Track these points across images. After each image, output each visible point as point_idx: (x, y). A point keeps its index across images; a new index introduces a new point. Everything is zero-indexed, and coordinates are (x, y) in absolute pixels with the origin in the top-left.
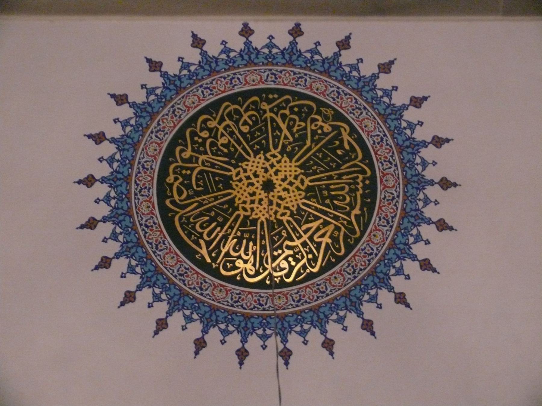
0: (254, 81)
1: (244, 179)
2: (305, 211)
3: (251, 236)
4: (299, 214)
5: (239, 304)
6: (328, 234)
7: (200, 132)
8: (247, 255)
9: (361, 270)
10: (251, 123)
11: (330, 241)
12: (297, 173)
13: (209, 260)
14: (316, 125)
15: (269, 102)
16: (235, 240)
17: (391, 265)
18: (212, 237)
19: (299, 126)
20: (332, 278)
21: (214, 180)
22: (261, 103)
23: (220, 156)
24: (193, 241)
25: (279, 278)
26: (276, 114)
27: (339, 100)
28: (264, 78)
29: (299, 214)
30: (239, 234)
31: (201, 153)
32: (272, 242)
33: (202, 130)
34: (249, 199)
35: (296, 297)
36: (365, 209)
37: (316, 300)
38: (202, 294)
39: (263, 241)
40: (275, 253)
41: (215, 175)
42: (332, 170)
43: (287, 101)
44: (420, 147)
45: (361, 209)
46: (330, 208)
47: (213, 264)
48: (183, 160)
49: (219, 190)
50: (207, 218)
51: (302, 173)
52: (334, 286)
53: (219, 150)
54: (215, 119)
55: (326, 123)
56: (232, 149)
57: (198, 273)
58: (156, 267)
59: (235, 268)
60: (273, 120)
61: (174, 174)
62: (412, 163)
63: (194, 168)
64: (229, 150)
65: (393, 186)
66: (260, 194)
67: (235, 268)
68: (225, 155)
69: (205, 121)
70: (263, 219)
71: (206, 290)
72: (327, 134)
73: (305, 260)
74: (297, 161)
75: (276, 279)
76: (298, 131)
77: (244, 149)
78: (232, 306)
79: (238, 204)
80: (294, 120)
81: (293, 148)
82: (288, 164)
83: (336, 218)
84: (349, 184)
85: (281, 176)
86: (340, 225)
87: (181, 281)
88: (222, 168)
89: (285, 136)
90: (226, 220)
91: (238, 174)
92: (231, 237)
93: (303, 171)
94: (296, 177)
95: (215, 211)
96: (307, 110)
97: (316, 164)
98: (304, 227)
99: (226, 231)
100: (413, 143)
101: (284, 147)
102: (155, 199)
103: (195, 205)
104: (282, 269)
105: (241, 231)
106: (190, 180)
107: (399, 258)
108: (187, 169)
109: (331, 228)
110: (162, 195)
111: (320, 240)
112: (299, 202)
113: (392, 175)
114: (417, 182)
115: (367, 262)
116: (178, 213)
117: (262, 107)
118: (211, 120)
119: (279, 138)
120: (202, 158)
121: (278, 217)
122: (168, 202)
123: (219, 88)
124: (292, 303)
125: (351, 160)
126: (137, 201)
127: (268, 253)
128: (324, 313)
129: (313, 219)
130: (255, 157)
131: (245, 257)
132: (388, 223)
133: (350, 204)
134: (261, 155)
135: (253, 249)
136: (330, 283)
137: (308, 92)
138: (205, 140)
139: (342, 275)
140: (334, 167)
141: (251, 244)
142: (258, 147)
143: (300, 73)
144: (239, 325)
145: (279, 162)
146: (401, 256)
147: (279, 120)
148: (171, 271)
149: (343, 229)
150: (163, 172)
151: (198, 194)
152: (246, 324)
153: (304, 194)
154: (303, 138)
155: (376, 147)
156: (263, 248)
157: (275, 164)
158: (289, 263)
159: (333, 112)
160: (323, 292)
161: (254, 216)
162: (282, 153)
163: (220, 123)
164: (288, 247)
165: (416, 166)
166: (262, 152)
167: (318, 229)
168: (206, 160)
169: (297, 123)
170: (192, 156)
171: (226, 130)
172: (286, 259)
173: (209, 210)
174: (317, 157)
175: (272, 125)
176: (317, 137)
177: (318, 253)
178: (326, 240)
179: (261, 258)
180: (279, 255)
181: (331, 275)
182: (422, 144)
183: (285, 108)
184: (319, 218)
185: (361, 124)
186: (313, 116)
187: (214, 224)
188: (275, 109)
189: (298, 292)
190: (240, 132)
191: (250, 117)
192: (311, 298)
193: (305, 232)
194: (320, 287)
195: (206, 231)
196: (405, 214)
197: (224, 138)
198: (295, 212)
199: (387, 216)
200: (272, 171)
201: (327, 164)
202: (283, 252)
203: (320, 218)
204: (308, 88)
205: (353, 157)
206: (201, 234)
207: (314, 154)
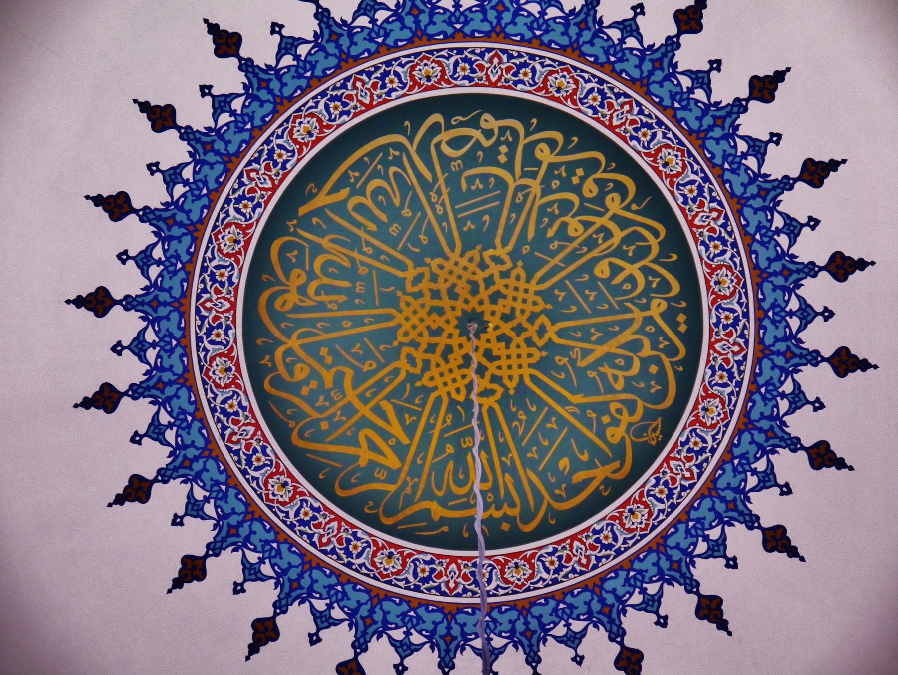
0: (718, 283)
1: (486, 274)
2: (423, 405)
3: (358, 296)
4: (415, 392)
5: (209, 283)
6: (375, 457)
7: (596, 181)
8: (317, 293)
9: (310, 536)
11: (362, 463)
12: (506, 381)
13: (302, 210)
14: (619, 411)
15: (669, 316)
16: (346, 264)
17: (334, 599)
18: (353, 214)
20: (283, 478)
21: (483, 213)
22: (668, 300)
23: (539, 222)
24: (345, 175)
25: (270, 365)
27: (684, 454)
28: (725, 303)
29: (415, 392)
30: (363, 271)
31: (546, 181)
32: (348, 343)
34: (443, 287)
35: (231, 406)
36: (445, 529)
37: (230, 450)
38: (228, 201)
39: (349, 324)
40: (324, 351)
41: (495, 214)
42: (522, 452)
44: (608, 626)
45: (443, 521)
46: (435, 455)
47: (295, 221)
48: (530, 148)
49: (461, 223)
50: (397, 201)
51: (507, 389)
52: (266, 483)
53: (553, 218)
54: (627, 208)
55: (627, 431)
56: (554, 246)
57: (274, 189)
58: (292, 100)
61: (500, 128)
62: (570, 613)
64: (552, 240)
65: (506, 581)
66: (453, 308)
67: (287, 268)
68: (541, 233)
69: (620, 189)
70: (399, 318)
71: (237, 210)
72: (601, 434)
74: (533, 378)
75: (267, 358)
76: (603, 376)
78: (204, 269)
79: (429, 265)
80: (628, 365)
82: (525, 361)
83: (415, 471)
85: (498, 349)
86: (399, 483)
87: (257, 155)
88: (509, 229)
89: (592, 351)
90: (393, 242)
91: (497, 260)
93: (512, 392)
94: (495, 379)
95: (414, 216)
96: (652, 391)
98: (387, 407)
99: (368, 244)
100: (614, 610)
101: (565, 351)
102: (446, 91)
104: (290, 369)
105: (370, 274)
108: (511, 155)
109: (392, 461)
113: (532, 576)
114: (528, 629)
115: (329, 548)
116: (411, 140)
117: (654, 302)
118: (622, 200)
119: (586, 339)
120: (535, 186)
121: (405, 350)
122: (437, 118)
123: (701, 214)
124: (219, 399)
125: (550, 488)
126: (444, 53)
128: (205, 469)
129: (408, 423)
130: (537, 293)
131: (311, 290)
133: (450, 495)
135: (330, 302)
136: (271, 476)
138: (577, 189)
139: (292, 499)
140: (529, 455)
141: (343, 298)
142: (560, 299)
143: (741, 373)
144: (162, 289)
145: (529, 342)
146: (358, 617)
147: (628, 336)
148: (280, 131)
149: (392, 488)
151: (453, 180)
152: (165, 304)
153: (461, 398)
154: (588, 387)
155: (587, 537)
156: (335, 324)
157: (524, 335)
158: (306, 382)
159: (654, 443)
160: (249, 463)
162: (550, 346)
163: (615, 218)
164: (339, 379)
165: (563, 622)
166: (549, 306)
167: (385, 435)
168: (529, 193)
169: (620, 374)
170: (539, 163)
171: (597, 232)
173: (416, 206)
174: (547, 419)
175: (612, 324)
176: (593, 415)
178: (365, 456)
179: (312, 322)
180: (320, 360)
181: (290, 475)
182: (615, 628)
183: (654, 347)
184: (411, 436)
185: (635, 501)
186: (640, 404)
187: (383, 217)
188: (650, 329)
189: (244, 409)
190: (596, 260)
191: (631, 279)
192: (235, 439)
193: (378, 411)
194: (259, 455)
195: (369, 202)
197: (581, 228)
198: (418, 384)
199: (439, 575)
200: (506, 328)
201: (534, 440)
202: (328, 368)
203: (411, 436)
204: (705, 390)
205: (557, 492)
207: (552, 412)
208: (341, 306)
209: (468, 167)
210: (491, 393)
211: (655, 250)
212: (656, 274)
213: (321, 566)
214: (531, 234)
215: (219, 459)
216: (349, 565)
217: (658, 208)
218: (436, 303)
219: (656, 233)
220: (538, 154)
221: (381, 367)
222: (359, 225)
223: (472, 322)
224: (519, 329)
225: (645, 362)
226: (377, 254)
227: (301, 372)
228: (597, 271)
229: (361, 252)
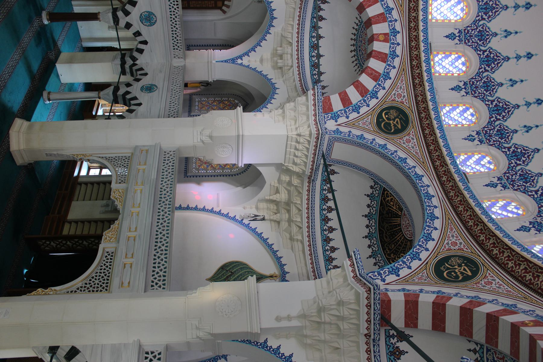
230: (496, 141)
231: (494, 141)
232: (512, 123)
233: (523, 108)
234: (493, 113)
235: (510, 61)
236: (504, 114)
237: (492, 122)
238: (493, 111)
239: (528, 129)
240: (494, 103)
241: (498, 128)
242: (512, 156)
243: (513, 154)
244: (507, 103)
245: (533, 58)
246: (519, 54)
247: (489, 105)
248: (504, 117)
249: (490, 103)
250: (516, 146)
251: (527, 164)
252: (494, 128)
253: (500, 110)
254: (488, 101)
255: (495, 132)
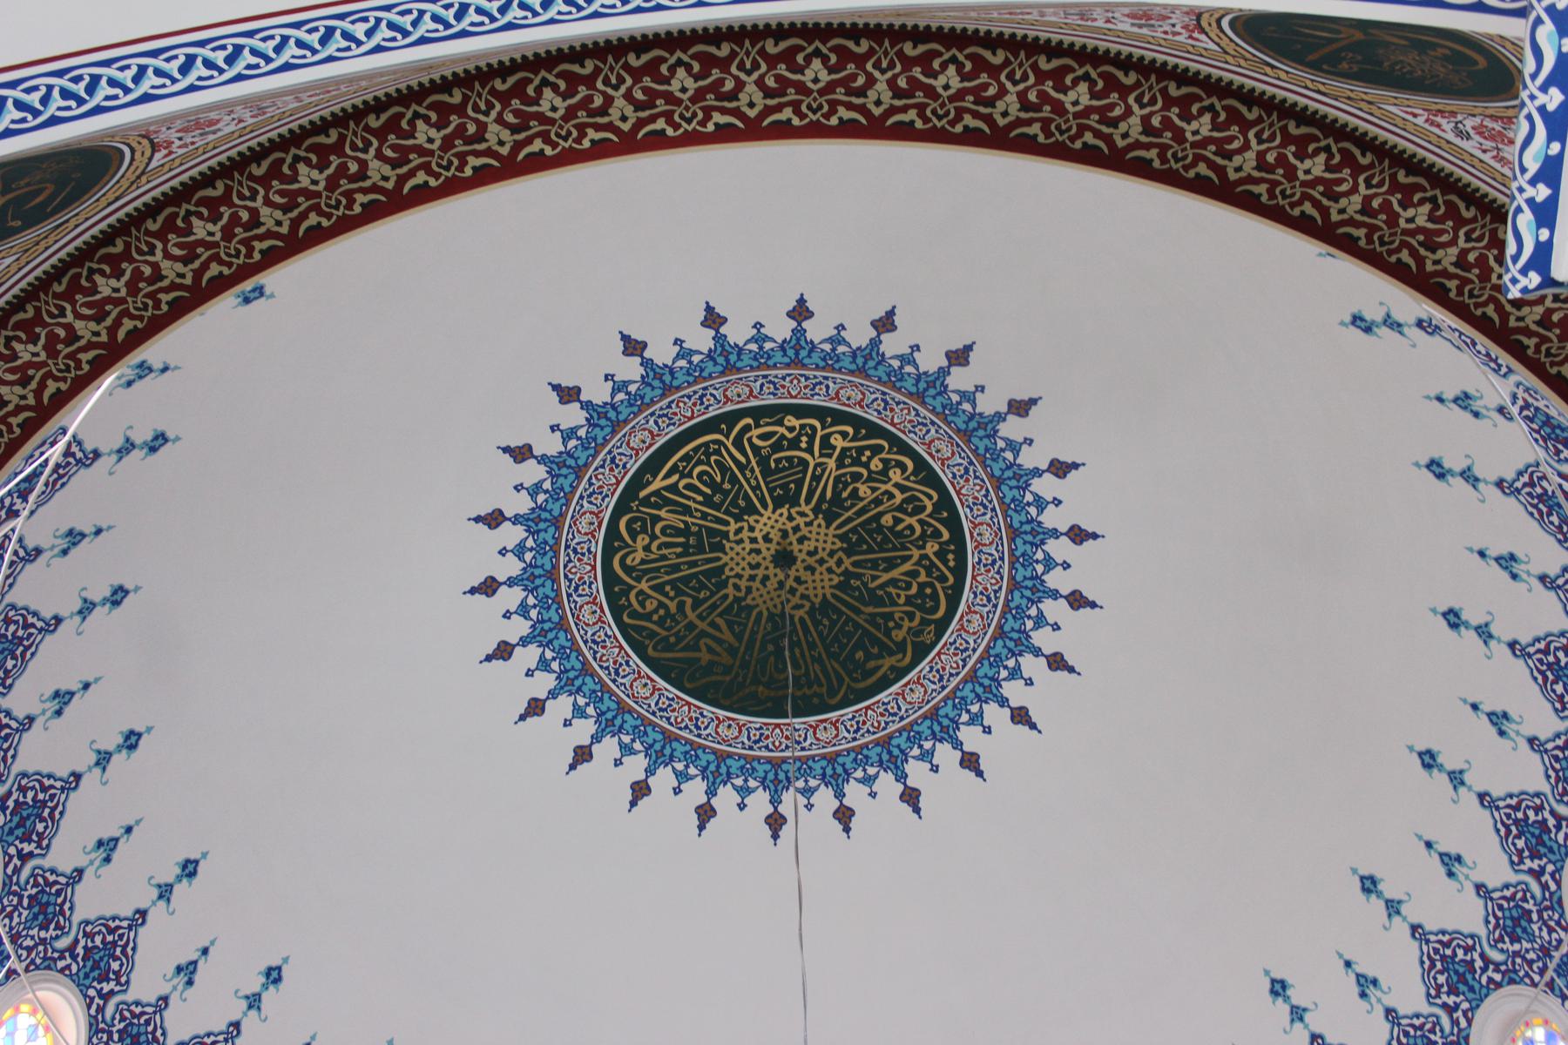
2: (748, 618)
4: (741, 609)
6: (716, 658)
8: (659, 548)
10: (899, 528)
11: (703, 663)
13: (642, 494)
14: (902, 619)
15: (941, 554)
19: (899, 596)
26: (918, 563)
29: (741, 609)
30: (694, 529)
32: (686, 580)
33: (885, 462)
40: (668, 588)
43: (943, 579)
49: (771, 491)
50: (718, 479)
53: (846, 485)
54: (907, 479)
59: (634, 535)
60: (906, 559)
63: (812, 454)
67: (634, 535)
68: (836, 493)
69: (903, 468)
73: (665, 633)
76: (889, 595)
77: (849, 520)
80: (909, 586)
81: (858, 588)
83: (744, 665)
84: (807, 673)
90: (717, 507)
92: (687, 519)
97: (833, 623)
101: (858, 576)
102: (754, 403)
103: (743, 460)
106: (789, 449)
107: (704, 770)
108: (811, 443)
110: (758, 413)
111: (704, 649)
112: (763, 607)
117: (929, 545)
120: (831, 463)
125: (849, 674)
127: (667, 578)
131: (654, 547)
132: (756, 742)
134: (839, 544)
137: (962, 607)
138: (866, 465)
141: (679, 550)
145: (830, 570)
147: (907, 567)
150: (800, 411)
151: (763, 462)
153: (778, 611)
156: (676, 568)
161: (728, 545)
162: (846, 573)
163: (896, 485)
164: (681, 605)
167: (720, 641)
170: (834, 448)
172: (661, 605)
173: (734, 480)
175: (896, 558)
177: (682, 650)
178: (705, 657)
179: (658, 569)
180: (666, 595)
183: (929, 574)
190: (881, 514)
191: (910, 527)
193: (713, 624)
196: (777, 764)
202: (672, 599)
206: (690, 475)
207: (849, 619)
208: (678, 556)
209: (774, 452)
210: (802, 606)
211: (929, 508)
212: (930, 525)
213: (677, 738)
214: (829, 494)
215: (593, 674)
216: (699, 736)
217: (933, 480)
218: (755, 546)
219: (930, 498)
220: (832, 441)
221: (713, 594)
222: (688, 498)
223: (784, 559)
224: (821, 562)
225: (922, 586)
226: (705, 516)
227: (650, 605)
228: (883, 521)
229: (691, 516)
230: (1545, 923)
231: (1551, 930)
232: (1469, 916)
233: (1412, 912)
234: (1477, 986)
235: (1317, 1031)
236: (1460, 953)
237: (1504, 974)
238: (1472, 989)
239: (1451, 862)
240: (1451, 1000)
241: (1507, 946)
242: (1551, 850)
243: (1543, 850)
244: (1428, 966)
245: (1278, 976)
246: (1288, 1018)
247: (1465, 1013)
248: (1468, 949)
249: (1460, 1013)
250: (1515, 859)
251: (1537, 795)
252: (1516, 954)
253: (1456, 972)
254: (1458, 1023)
255: (1526, 945)
